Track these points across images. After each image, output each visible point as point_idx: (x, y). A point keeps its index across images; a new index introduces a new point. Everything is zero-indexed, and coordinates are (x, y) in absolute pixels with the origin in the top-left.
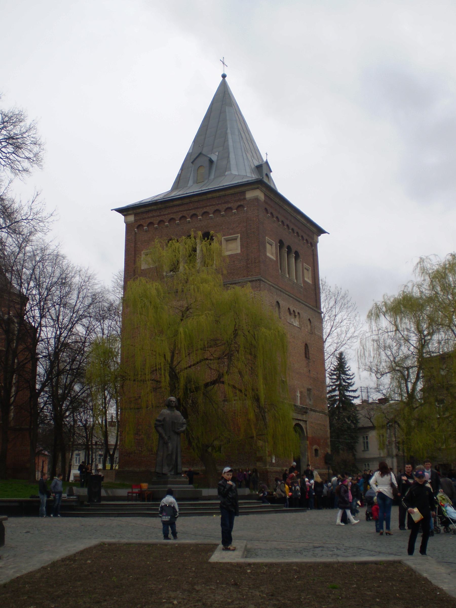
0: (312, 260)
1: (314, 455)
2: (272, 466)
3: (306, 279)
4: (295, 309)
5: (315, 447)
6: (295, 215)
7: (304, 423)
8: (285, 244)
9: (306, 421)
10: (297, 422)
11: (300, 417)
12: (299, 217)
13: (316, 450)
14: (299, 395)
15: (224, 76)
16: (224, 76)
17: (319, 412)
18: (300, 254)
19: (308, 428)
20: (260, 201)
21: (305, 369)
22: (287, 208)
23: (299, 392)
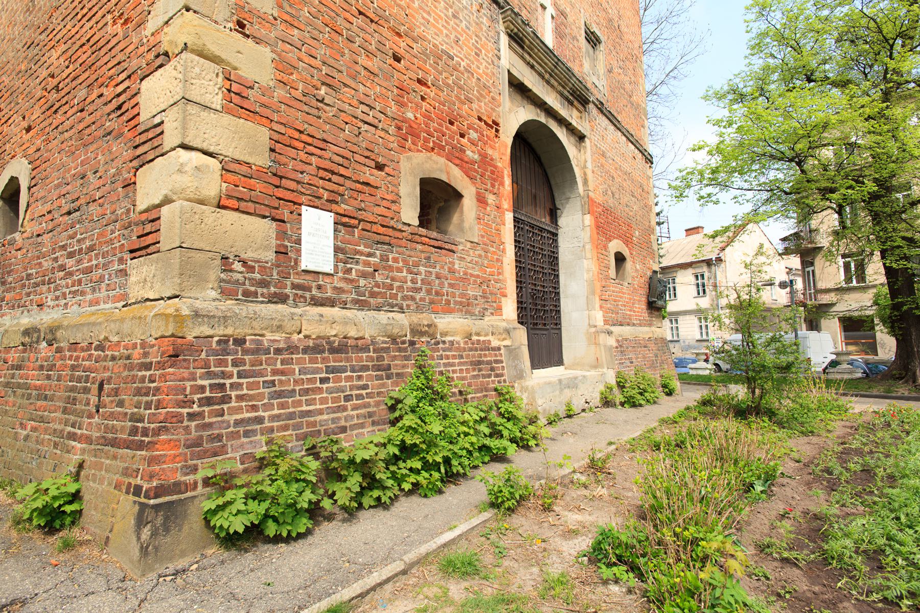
1: (612, 272)
2: (282, 299)
5: (615, 245)
10: (542, 118)
13: (620, 259)
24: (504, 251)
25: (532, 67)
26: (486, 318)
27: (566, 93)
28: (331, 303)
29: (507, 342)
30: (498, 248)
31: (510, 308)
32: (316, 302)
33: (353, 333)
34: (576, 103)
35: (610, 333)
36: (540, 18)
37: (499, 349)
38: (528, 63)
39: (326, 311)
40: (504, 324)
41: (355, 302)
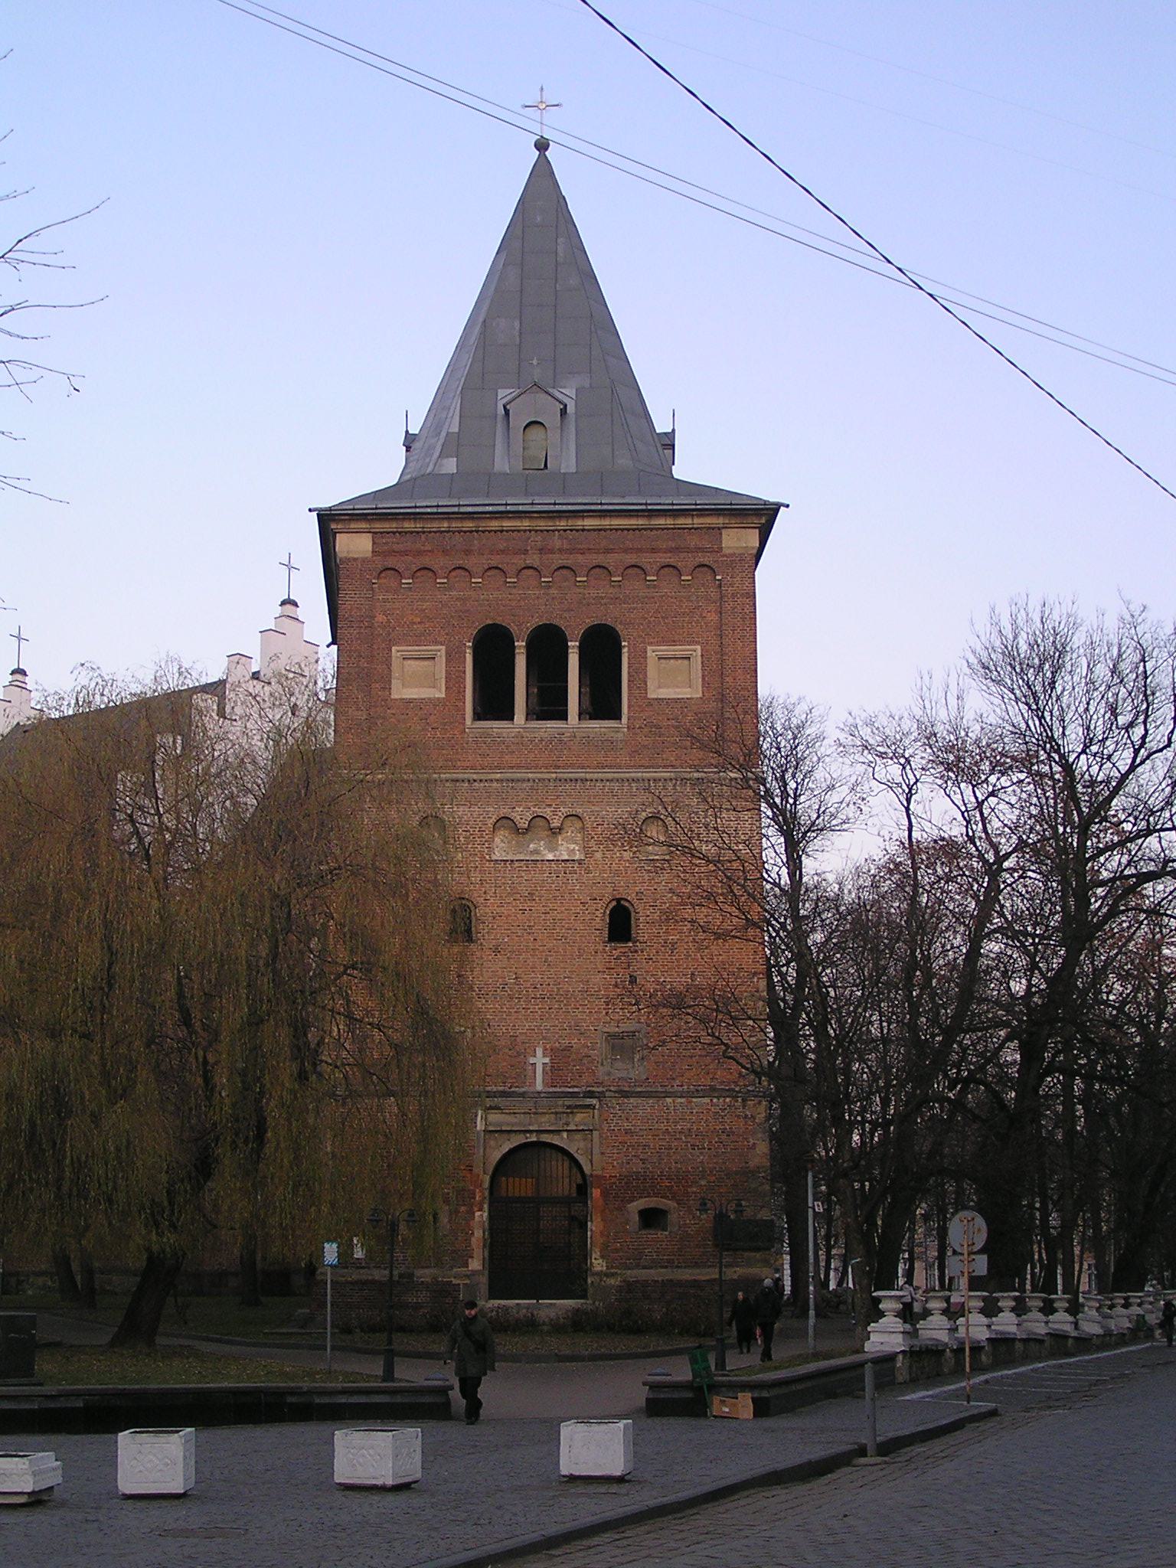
0: (713, 617)
2: (347, 1268)
3: (652, 695)
4: (547, 812)
6: (562, 524)
7: (578, 1136)
8: (514, 629)
9: (591, 1130)
11: (546, 1122)
12: (589, 523)
14: (540, 1060)
15: (542, 146)
16: (542, 146)
17: (689, 1095)
18: (619, 628)
19: (596, 1151)
20: (355, 559)
21: (597, 979)
22: (504, 525)
23: (539, 1051)
24: (473, 1234)
25: (515, 1113)
26: (455, 1270)
27: (561, 1110)
28: (363, 1268)
29: (468, 1282)
30: (467, 1233)
31: (475, 1265)
32: (358, 1268)
33: (370, 1278)
34: (575, 1111)
35: (613, 1275)
36: (530, 1073)
37: (459, 1284)
38: (510, 1113)
39: (362, 1271)
40: (469, 1273)
41: (374, 1267)
